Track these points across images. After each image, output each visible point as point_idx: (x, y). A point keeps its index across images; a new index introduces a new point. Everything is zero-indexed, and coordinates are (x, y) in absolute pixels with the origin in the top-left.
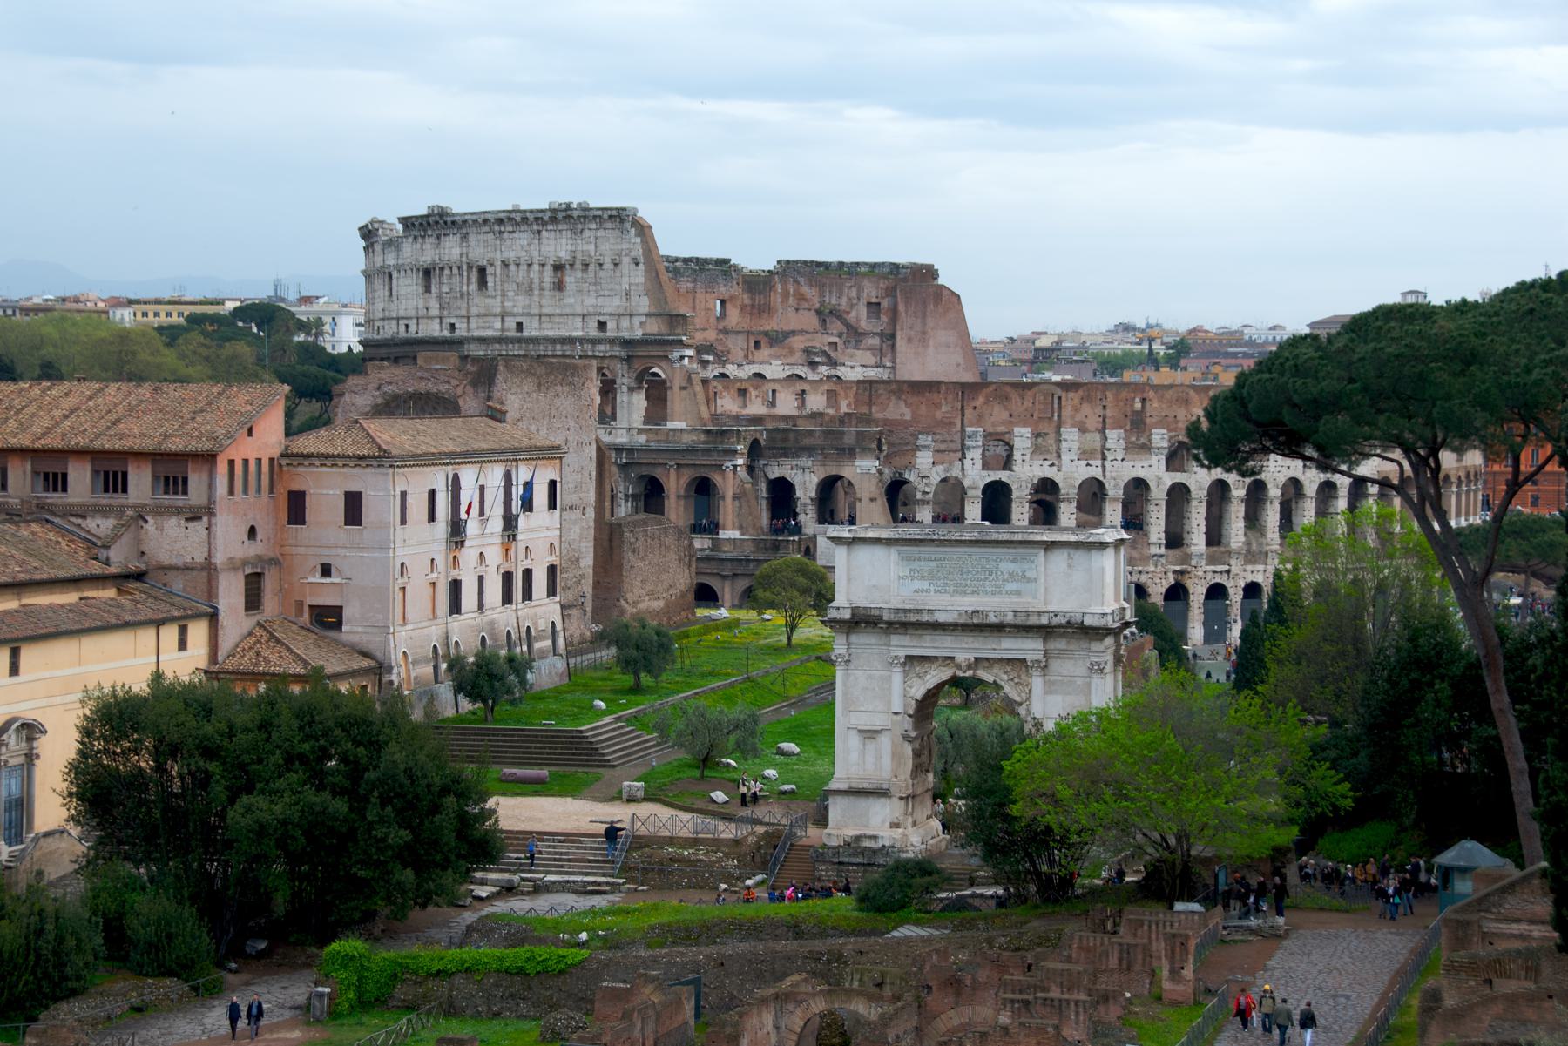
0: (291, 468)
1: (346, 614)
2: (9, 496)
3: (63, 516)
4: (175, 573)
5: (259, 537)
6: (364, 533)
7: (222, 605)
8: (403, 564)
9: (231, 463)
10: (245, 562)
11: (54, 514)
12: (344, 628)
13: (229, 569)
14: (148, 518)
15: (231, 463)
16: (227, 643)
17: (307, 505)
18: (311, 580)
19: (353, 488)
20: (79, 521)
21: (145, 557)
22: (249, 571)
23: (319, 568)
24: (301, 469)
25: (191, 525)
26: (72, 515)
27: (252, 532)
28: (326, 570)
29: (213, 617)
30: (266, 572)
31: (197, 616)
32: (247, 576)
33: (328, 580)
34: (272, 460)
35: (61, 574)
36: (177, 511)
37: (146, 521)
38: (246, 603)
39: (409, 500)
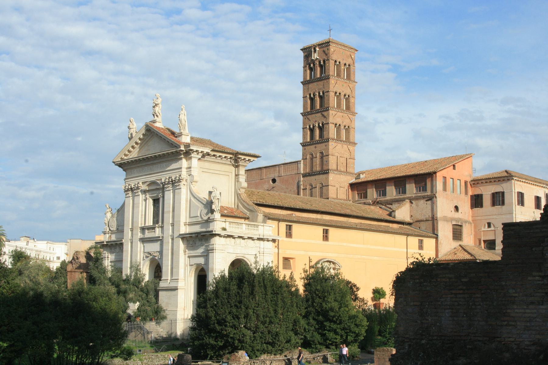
4: (423, 222)
5: (460, 211)
7: (440, 234)
10: (452, 219)
13: (444, 220)
18: (483, 229)
20: (390, 206)
21: (412, 217)
22: (454, 223)
26: (388, 204)
27: (457, 208)
30: (464, 225)
33: (490, 229)
36: (423, 197)
38: (453, 236)
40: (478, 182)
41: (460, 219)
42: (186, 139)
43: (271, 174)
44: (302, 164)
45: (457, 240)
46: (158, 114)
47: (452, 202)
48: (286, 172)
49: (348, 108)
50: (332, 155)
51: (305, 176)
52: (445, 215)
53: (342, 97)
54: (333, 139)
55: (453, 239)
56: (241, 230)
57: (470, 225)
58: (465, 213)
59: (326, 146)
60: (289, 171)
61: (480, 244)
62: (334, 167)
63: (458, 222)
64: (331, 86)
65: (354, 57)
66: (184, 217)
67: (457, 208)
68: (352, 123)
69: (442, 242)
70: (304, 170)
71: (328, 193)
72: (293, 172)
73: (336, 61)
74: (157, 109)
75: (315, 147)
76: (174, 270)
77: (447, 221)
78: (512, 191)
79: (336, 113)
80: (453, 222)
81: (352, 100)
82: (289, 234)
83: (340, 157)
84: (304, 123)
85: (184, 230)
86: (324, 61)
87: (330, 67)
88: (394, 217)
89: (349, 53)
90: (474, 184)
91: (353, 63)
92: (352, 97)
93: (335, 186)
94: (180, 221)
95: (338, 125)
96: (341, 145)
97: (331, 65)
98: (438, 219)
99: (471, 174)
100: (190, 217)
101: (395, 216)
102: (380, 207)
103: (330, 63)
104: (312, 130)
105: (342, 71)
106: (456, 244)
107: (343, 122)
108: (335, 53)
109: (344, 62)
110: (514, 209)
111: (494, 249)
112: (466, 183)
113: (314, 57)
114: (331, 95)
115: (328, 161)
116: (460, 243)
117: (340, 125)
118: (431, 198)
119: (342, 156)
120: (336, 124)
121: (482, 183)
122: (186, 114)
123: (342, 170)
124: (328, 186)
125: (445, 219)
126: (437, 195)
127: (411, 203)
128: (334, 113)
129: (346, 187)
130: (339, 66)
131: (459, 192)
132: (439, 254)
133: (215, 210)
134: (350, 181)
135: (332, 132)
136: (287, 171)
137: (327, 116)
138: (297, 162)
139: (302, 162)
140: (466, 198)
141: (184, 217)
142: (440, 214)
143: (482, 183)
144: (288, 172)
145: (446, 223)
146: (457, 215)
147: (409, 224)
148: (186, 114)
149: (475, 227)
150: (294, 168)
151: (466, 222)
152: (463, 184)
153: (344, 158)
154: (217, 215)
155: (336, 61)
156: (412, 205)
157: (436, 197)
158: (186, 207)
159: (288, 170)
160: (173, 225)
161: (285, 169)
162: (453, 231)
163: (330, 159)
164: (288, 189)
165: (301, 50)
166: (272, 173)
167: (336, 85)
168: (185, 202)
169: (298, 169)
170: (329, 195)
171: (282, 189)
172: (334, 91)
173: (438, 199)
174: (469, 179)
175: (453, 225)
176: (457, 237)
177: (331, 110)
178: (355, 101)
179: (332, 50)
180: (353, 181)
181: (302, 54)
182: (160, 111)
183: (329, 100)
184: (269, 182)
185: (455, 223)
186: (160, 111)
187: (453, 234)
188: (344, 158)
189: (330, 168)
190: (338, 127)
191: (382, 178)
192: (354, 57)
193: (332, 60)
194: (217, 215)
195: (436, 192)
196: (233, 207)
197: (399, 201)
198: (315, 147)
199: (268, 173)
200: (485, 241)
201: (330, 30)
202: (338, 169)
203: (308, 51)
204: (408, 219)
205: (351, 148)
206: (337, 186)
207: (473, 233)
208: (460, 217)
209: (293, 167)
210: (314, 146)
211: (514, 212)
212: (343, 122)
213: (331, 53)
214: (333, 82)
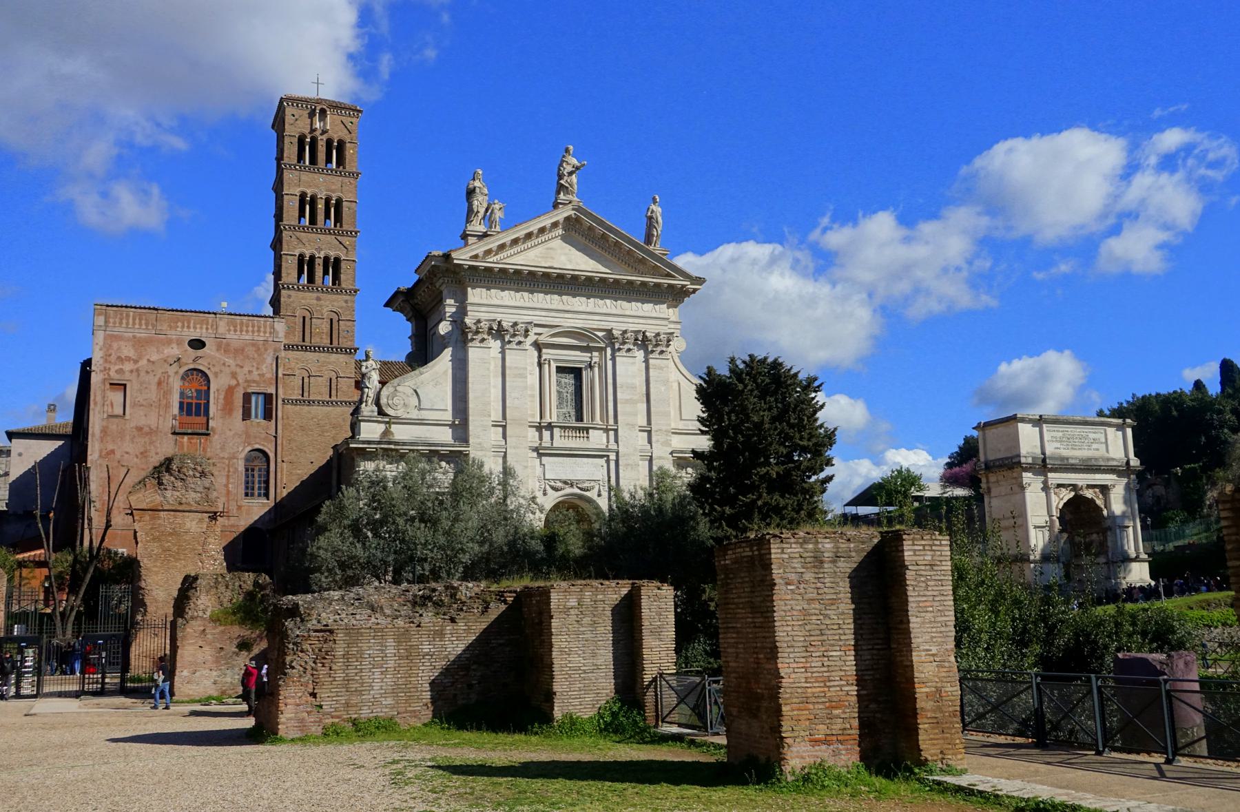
43: (189, 327)
48: (238, 333)
51: (288, 347)
59: (346, 302)
60: (247, 331)
72: (259, 336)
136: (241, 331)
137: (349, 248)
144: (244, 333)
150: (262, 329)
159: (245, 328)
164: (242, 367)
166: (192, 325)
171: (224, 364)
199: (180, 324)
209: (259, 327)
210: (315, 295)
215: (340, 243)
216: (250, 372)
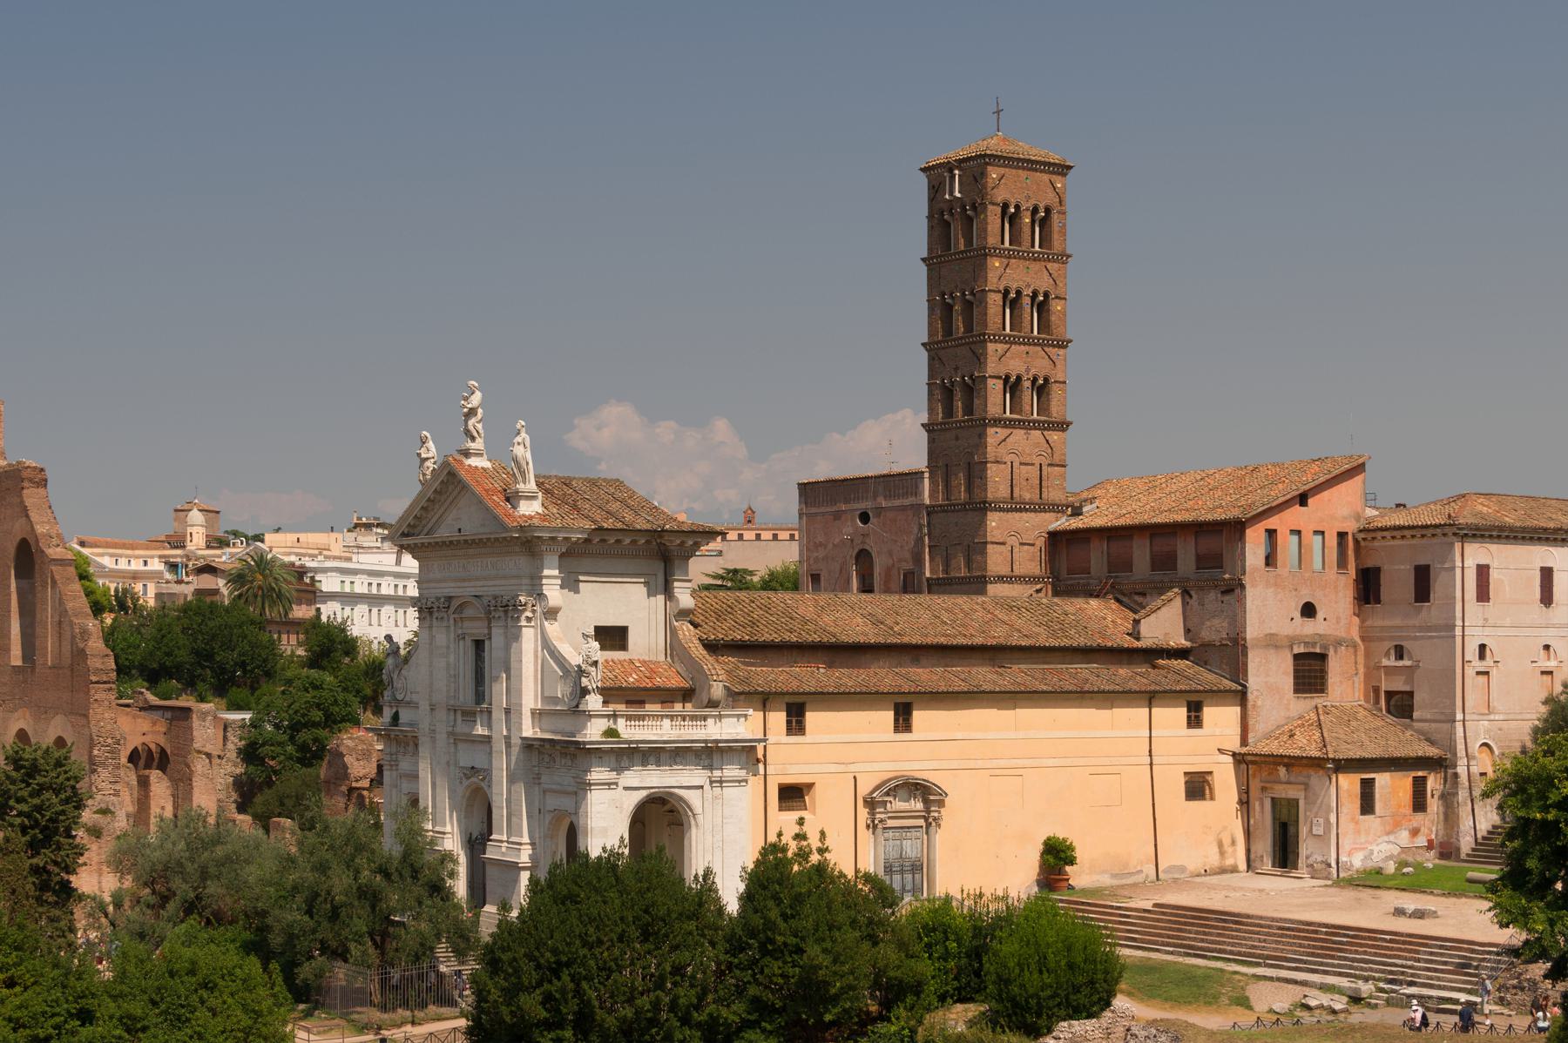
0: (1367, 543)
1: (1417, 698)
2: (1091, 578)
3: (1129, 595)
5: (1320, 615)
6: (1431, 612)
7: (1254, 682)
8: (1482, 647)
9: (1271, 533)
10: (1292, 641)
11: (1124, 595)
12: (1416, 715)
13: (1267, 646)
14: (1193, 593)
15: (1271, 533)
16: (1259, 727)
17: (1382, 582)
18: (1385, 662)
19: (1423, 562)
20: (1139, 599)
22: (1296, 651)
23: (1393, 652)
24: (1376, 544)
25: (1227, 598)
27: (1309, 610)
28: (1400, 653)
29: (1241, 697)
30: (1331, 653)
31: (1219, 696)
32: (1297, 657)
33: (1400, 663)
34: (1342, 536)
35: (1065, 642)
37: (1191, 597)
39: (1494, 575)
40: (1373, 535)
41: (1320, 635)
42: (530, 508)
44: (926, 481)
45: (1310, 692)
46: (475, 434)
47: (1294, 593)
49: (1044, 325)
50: (998, 462)
52: (1272, 632)
53: (1026, 301)
54: (997, 422)
55: (1296, 691)
56: (659, 732)
57: (1351, 650)
58: (1338, 619)
61: (1377, 702)
62: (1004, 492)
63: (1314, 646)
64: (990, 275)
65: (1064, 186)
66: (530, 699)
67: (1309, 610)
68: (1058, 366)
69: (1259, 703)
70: (931, 496)
71: (986, 562)
73: (1005, 206)
74: (471, 422)
75: (957, 438)
76: (514, 819)
77: (1276, 647)
78: (1453, 568)
79: (1008, 346)
80: (1295, 647)
81: (1056, 306)
82: (796, 725)
83: (1021, 464)
84: (931, 375)
85: (528, 730)
86: (974, 208)
87: (987, 224)
88: (1138, 639)
89: (1046, 177)
90: (1364, 539)
91: (1060, 202)
92: (1057, 297)
93: (1003, 544)
94: (521, 705)
95: (1013, 379)
96: (1023, 432)
97: (990, 219)
98: (1249, 644)
99: (1359, 510)
100: (545, 699)
101: (1139, 633)
102: (1118, 600)
103: (989, 214)
104: (948, 393)
105: (1026, 230)
106: (1303, 705)
107: (1028, 370)
108: (1005, 187)
109: (1030, 205)
110: (1458, 614)
111: (1411, 717)
112: (1342, 536)
113: (951, 193)
114: (990, 302)
115: (983, 477)
116: (1319, 700)
117: (1019, 378)
118: (1234, 588)
119: (1028, 460)
120: (1007, 378)
121: (1383, 538)
122: (528, 444)
123: (1027, 496)
124: (986, 543)
125: (1272, 642)
126: (1247, 581)
127: (1186, 593)
128: (1001, 347)
129: (1041, 542)
130: (1014, 219)
131: (1317, 564)
132: (1250, 735)
133: (590, 687)
134: (1051, 523)
135: (995, 400)
138: (916, 476)
139: (927, 475)
140: (1342, 578)
141: (530, 699)
142: (1252, 632)
143: (1383, 538)
145: (1272, 651)
146: (1310, 628)
147: (1181, 653)
148: (528, 444)
149: (1367, 655)
151: (1338, 643)
152: (1332, 541)
153: (1033, 464)
154: (594, 702)
155: (1005, 206)
156: (1191, 602)
157: (1243, 587)
158: (536, 671)
160: (508, 711)
161: (890, 491)
162: (1296, 671)
163: (989, 472)
165: (923, 170)
167: (1007, 271)
168: (532, 659)
169: (916, 491)
170: (989, 568)
172: (1001, 288)
173: (1250, 592)
174: (1351, 527)
175: (1297, 657)
176: (1310, 684)
177: (991, 341)
178: (1064, 308)
179: (994, 176)
180: (1062, 523)
181: (923, 181)
182: (479, 426)
183: (986, 314)
184: (853, 520)
185: (1302, 650)
186: (479, 426)
187: (1296, 677)
188: (1033, 464)
189: (990, 496)
190: (1012, 386)
191: (1121, 522)
192: (1064, 186)
193: (994, 204)
194: (594, 702)
195: (1244, 573)
196: (662, 658)
197: (1161, 589)
198: (957, 438)
200: (1389, 694)
201: (998, 112)
202: (1015, 495)
203: (937, 175)
204: (1179, 640)
205: (1054, 436)
206: (1013, 541)
207: (1362, 670)
208: (1321, 632)
211: (1459, 623)
212: (1028, 370)
213: (990, 185)
214: (997, 264)
215: (974, 353)
216: (902, 547)
